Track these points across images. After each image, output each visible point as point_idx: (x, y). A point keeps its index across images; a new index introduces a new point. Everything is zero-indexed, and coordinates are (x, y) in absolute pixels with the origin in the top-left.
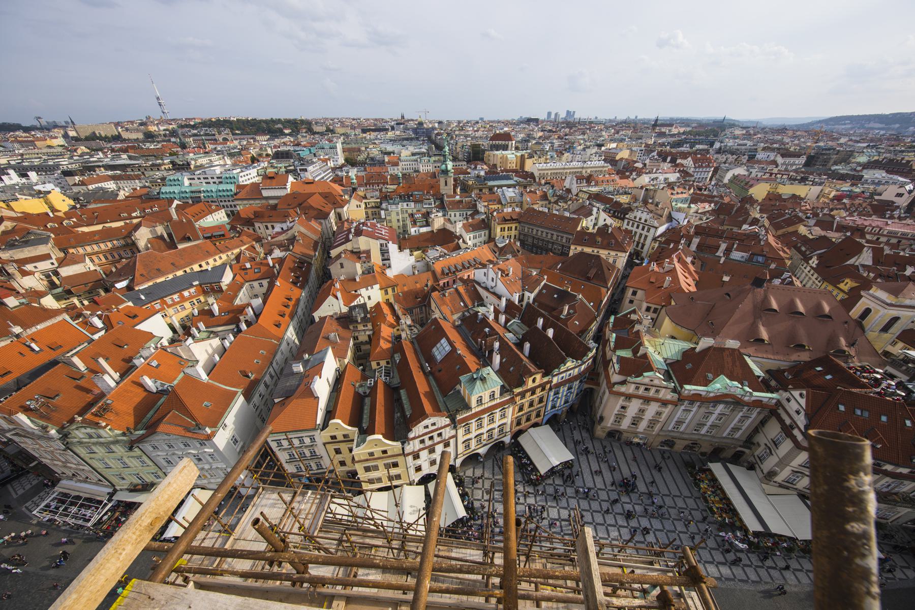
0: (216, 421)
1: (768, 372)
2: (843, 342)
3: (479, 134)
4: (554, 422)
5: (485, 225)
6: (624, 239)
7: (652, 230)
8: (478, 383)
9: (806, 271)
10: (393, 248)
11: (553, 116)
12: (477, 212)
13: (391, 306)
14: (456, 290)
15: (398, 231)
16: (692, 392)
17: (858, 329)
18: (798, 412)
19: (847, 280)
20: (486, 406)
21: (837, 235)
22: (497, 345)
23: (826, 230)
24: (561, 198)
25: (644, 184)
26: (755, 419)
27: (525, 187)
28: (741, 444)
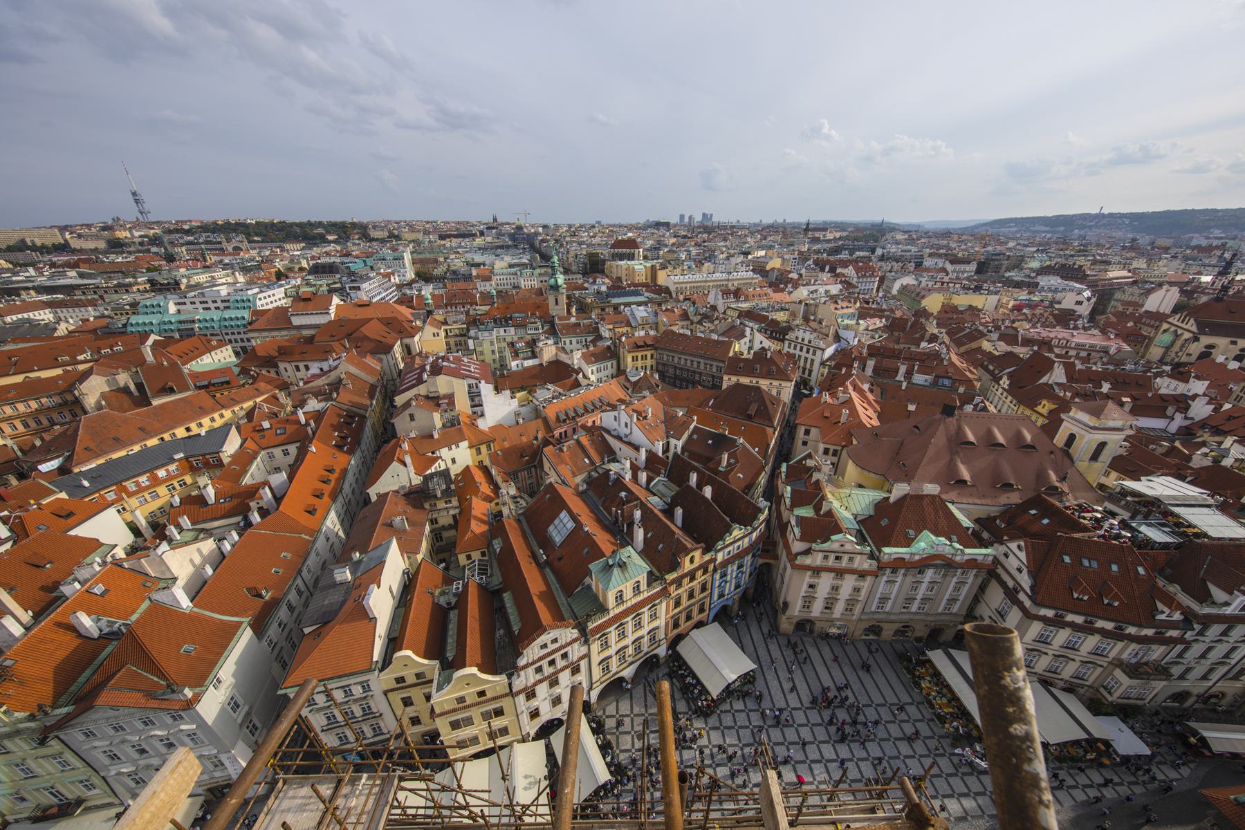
0: (201, 675)
2: (1053, 476)
3: (596, 240)
4: (724, 617)
5: (611, 353)
6: (787, 365)
7: (819, 353)
8: (616, 571)
9: (998, 393)
10: (486, 389)
11: (686, 220)
12: (600, 337)
13: (486, 471)
14: (578, 442)
15: (494, 366)
18: (1020, 570)
19: (1044, 402)
20: (629, 604)
24: (705, 317)
26: (973, 583)
27: (660, 305)
28: (962, 619)
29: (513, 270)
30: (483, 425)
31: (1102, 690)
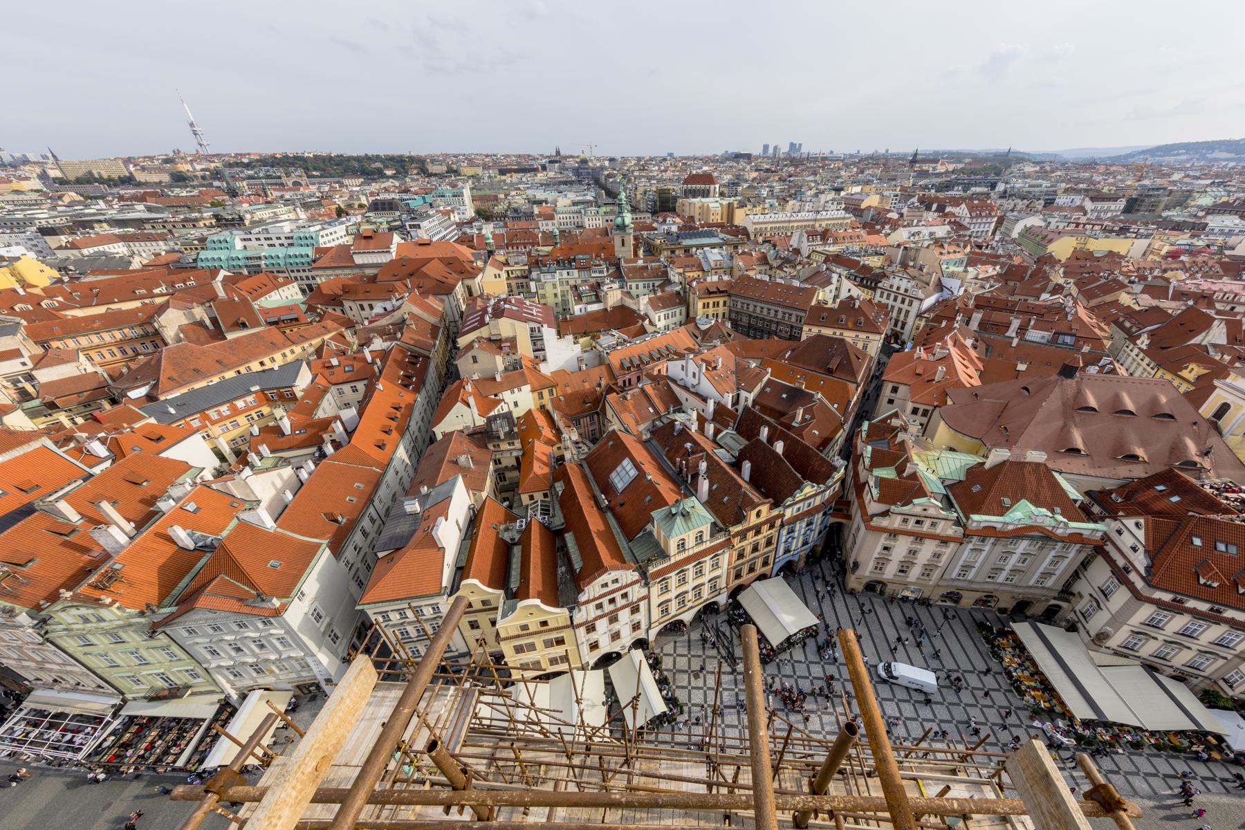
3: (669, 174)
5: (681, 299)
6: (878, 314)
10: (549, 333)
11: (771, 151)
12: (668, 282)
14: (643, 390)
15: (556, 310)
16: (983, 525)
17: (1213, 432)
19: (1192, 366)
21: (1174, 304)
22: (703, 466)
25: (901, 241)
26: (1074, 558)
27: (736, 247)
29: (576, 208)
30: (546, 369)
31: (1222, 683)
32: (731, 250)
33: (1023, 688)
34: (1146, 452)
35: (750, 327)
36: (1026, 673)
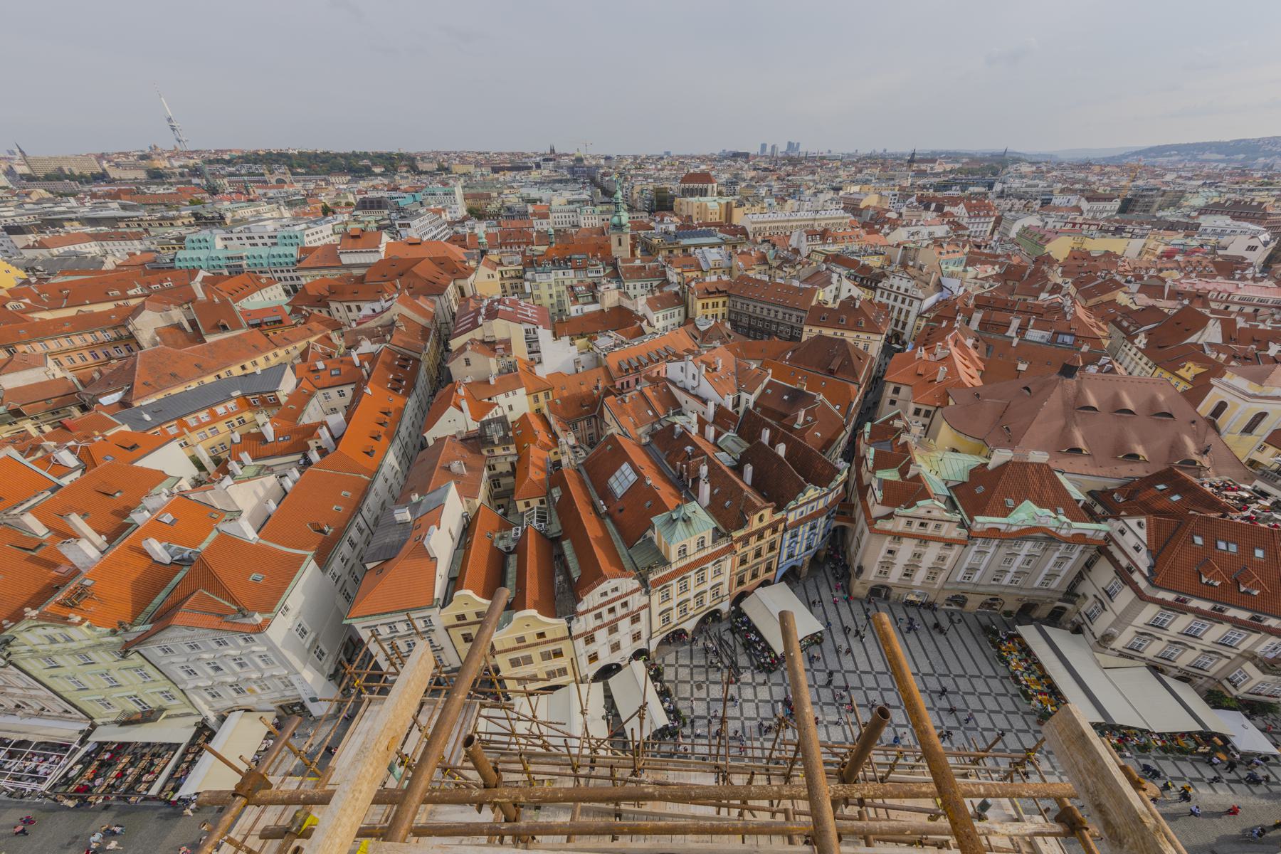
1: (1090, 494)
3: (666, 173)
5: (680, 300)
6: (878, 314)
8: (680, 525)
9: (1131, 353)
10: (544, 335)
11: (769, 150)
12: (666, 282)
13: (544, 419)
14: (641, 393)
16: (987, 526)
17: (1210, 429)
19: (1189, 364)
21: (1170, 304)
22: (704, 470)
23: (1155, 298)
25: (901, 240)
26: (1078, 560)
27: (735, 247)
29: (571, 207)
31: (1226, 683)
32: (730, 249)
33: (1030, 692)
34: (1146, 450)
35: (750, 327)
36: (1033, 677)
